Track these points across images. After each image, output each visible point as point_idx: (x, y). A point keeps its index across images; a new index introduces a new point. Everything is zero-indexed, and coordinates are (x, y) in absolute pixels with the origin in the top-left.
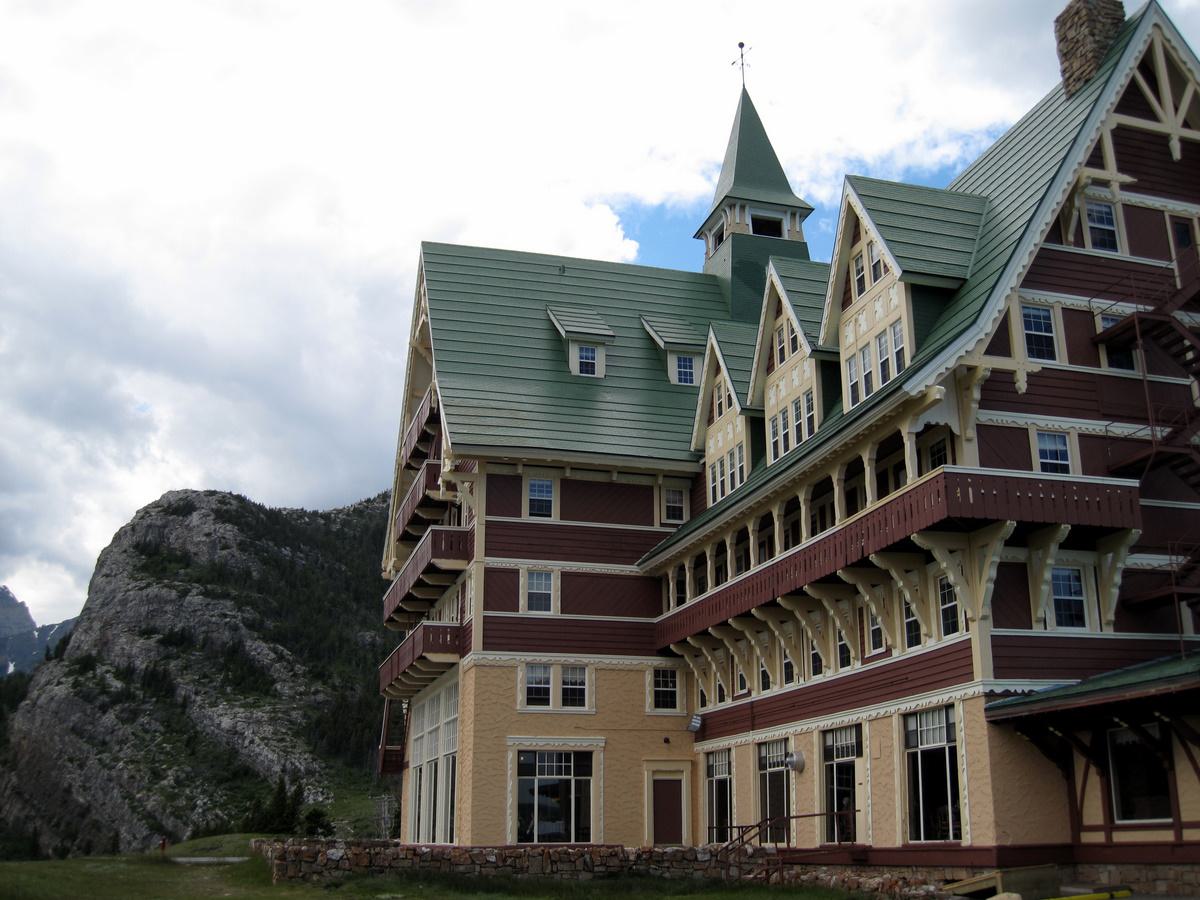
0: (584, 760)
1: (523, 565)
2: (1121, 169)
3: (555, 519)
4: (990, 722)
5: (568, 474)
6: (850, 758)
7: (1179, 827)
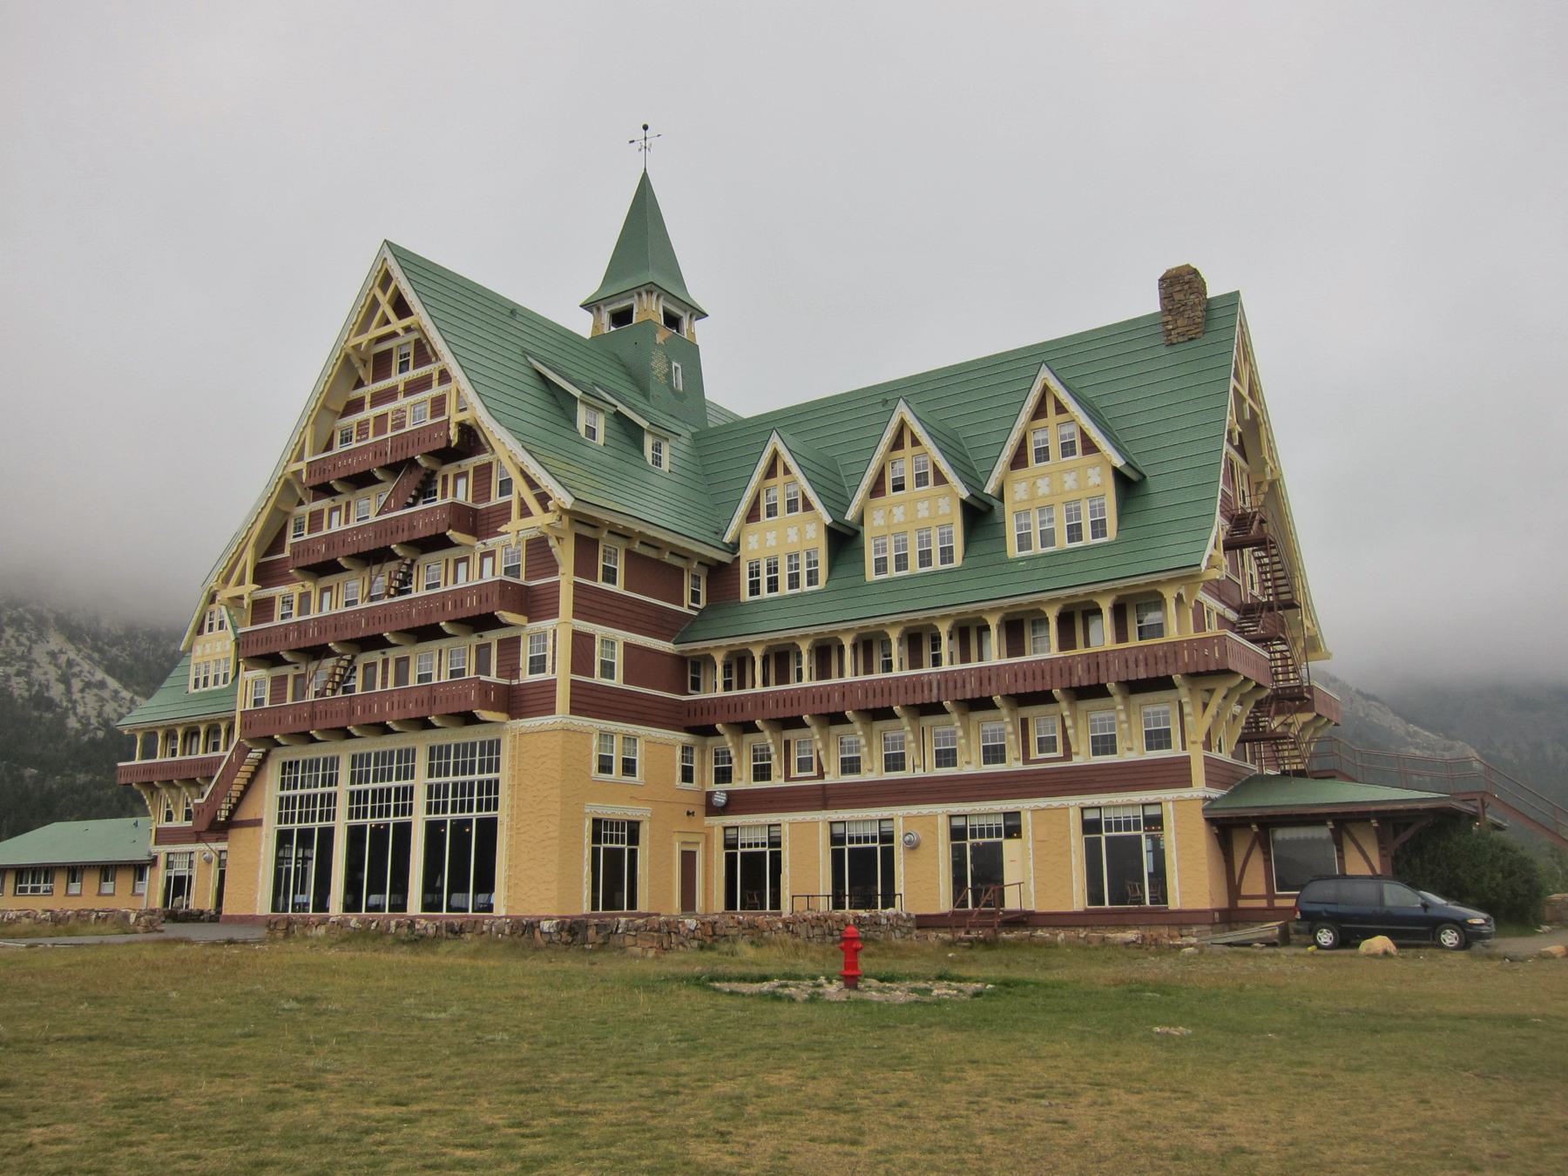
0: (634, 829)
1: (599, 631)
3: (618, 588)
4: (1206, 819)
5: (637, 547)
6: (995, 839)
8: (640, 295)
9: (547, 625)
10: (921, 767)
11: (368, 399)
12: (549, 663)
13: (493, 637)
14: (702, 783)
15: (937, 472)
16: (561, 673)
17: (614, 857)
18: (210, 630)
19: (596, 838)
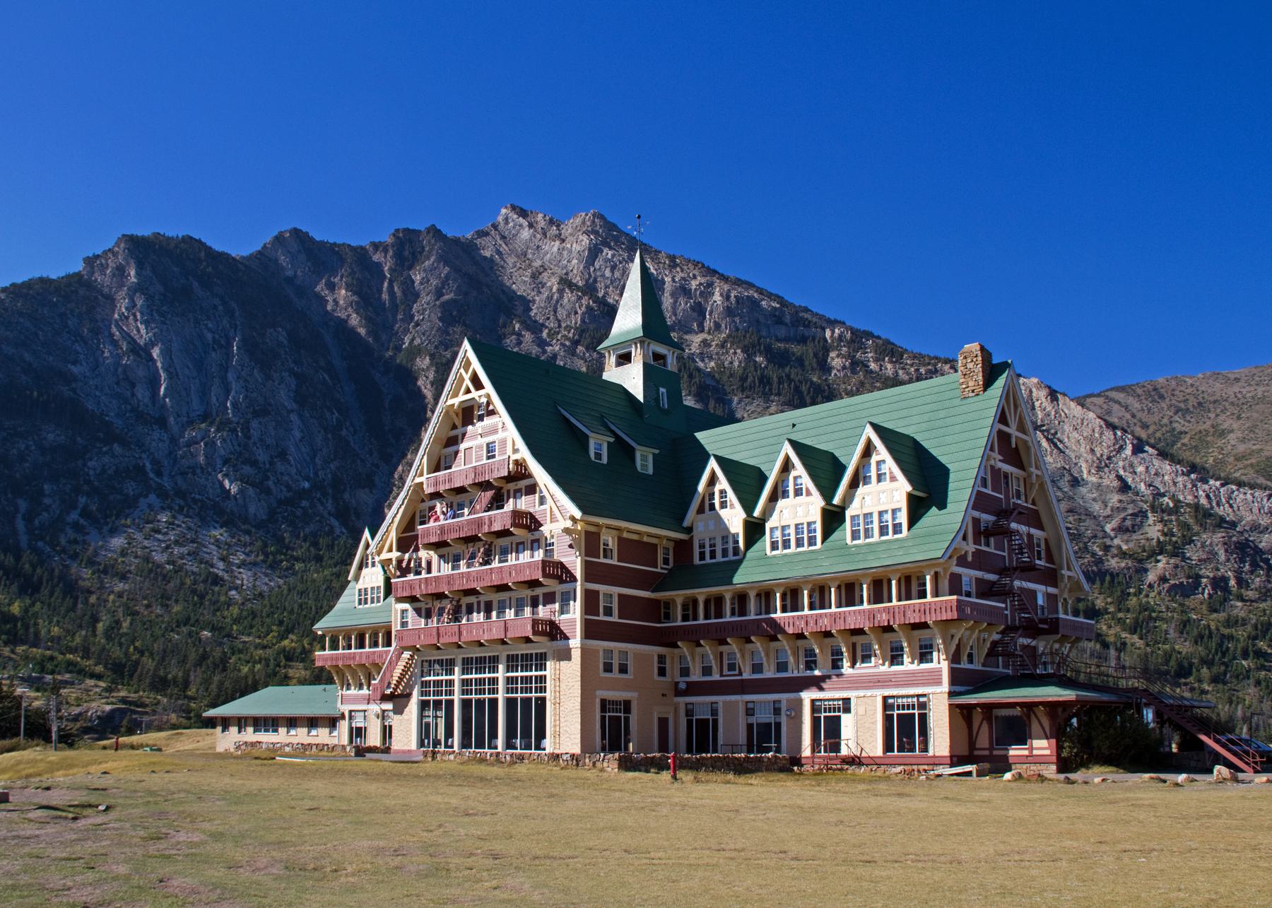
0: (627, 706)
1: (602, 588)
5: (625, 535)
6: (837, 714)
7: (1031, 749)
8: (636, 344)
15: (807, 490)
19: (603, 709)
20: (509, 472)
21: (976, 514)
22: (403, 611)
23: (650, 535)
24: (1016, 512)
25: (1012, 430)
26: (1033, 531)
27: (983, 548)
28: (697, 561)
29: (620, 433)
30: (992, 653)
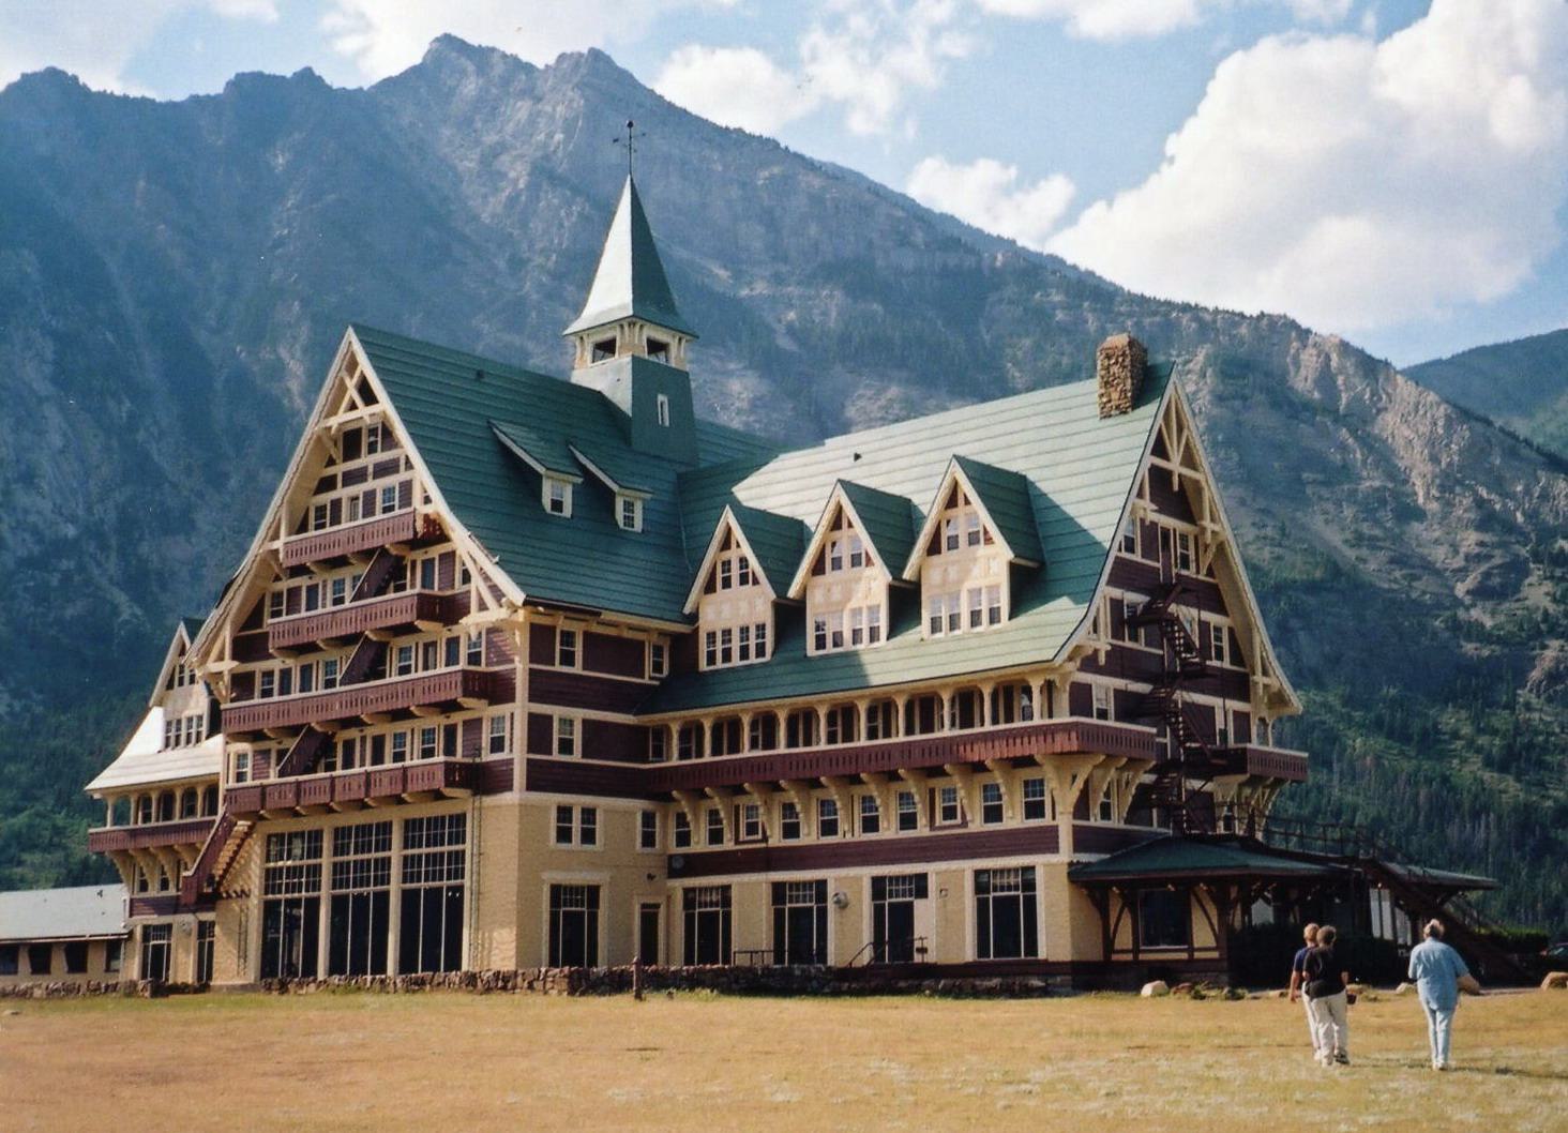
0: (594, 891)
1: (556, 711)
2: (1152, 501)
3: (577, 669)
6: (908, 899)
7: (1191, 950)
9: (503, 709)
10: (850, 832)
11: (340, 479)
12: (507, 743)
13: (457, 718)
14: (665, 845)
16: (517, 754)
17: (574, 920)
18: (181, 683)
20: (416, 533)
21: (1117, 593)
22: (241, 757)
23: (631, 628)
24: (1179, 588)
25: (1175, 465)
26: (1207, 616)
27: (1128, 644)
28: (703, 666)
29: (592, 468)
30: (1141, 804)
